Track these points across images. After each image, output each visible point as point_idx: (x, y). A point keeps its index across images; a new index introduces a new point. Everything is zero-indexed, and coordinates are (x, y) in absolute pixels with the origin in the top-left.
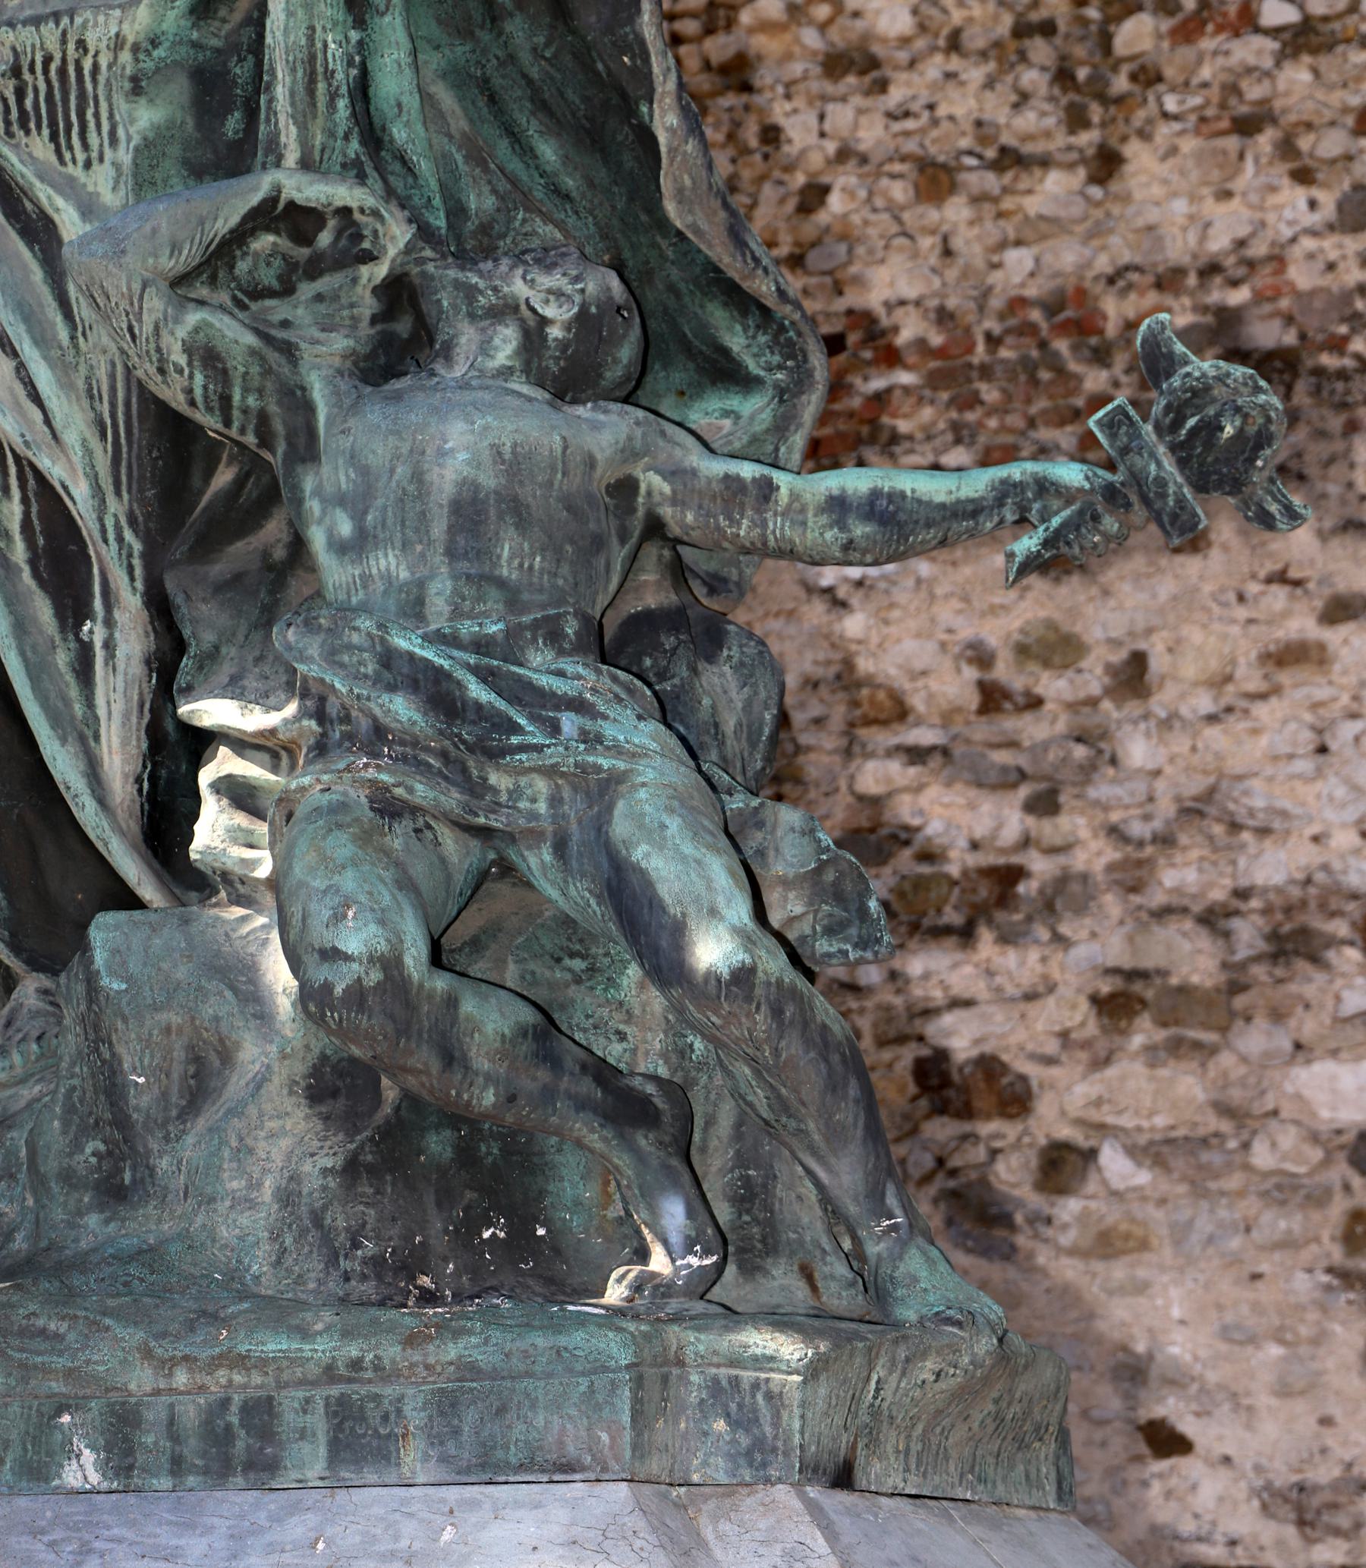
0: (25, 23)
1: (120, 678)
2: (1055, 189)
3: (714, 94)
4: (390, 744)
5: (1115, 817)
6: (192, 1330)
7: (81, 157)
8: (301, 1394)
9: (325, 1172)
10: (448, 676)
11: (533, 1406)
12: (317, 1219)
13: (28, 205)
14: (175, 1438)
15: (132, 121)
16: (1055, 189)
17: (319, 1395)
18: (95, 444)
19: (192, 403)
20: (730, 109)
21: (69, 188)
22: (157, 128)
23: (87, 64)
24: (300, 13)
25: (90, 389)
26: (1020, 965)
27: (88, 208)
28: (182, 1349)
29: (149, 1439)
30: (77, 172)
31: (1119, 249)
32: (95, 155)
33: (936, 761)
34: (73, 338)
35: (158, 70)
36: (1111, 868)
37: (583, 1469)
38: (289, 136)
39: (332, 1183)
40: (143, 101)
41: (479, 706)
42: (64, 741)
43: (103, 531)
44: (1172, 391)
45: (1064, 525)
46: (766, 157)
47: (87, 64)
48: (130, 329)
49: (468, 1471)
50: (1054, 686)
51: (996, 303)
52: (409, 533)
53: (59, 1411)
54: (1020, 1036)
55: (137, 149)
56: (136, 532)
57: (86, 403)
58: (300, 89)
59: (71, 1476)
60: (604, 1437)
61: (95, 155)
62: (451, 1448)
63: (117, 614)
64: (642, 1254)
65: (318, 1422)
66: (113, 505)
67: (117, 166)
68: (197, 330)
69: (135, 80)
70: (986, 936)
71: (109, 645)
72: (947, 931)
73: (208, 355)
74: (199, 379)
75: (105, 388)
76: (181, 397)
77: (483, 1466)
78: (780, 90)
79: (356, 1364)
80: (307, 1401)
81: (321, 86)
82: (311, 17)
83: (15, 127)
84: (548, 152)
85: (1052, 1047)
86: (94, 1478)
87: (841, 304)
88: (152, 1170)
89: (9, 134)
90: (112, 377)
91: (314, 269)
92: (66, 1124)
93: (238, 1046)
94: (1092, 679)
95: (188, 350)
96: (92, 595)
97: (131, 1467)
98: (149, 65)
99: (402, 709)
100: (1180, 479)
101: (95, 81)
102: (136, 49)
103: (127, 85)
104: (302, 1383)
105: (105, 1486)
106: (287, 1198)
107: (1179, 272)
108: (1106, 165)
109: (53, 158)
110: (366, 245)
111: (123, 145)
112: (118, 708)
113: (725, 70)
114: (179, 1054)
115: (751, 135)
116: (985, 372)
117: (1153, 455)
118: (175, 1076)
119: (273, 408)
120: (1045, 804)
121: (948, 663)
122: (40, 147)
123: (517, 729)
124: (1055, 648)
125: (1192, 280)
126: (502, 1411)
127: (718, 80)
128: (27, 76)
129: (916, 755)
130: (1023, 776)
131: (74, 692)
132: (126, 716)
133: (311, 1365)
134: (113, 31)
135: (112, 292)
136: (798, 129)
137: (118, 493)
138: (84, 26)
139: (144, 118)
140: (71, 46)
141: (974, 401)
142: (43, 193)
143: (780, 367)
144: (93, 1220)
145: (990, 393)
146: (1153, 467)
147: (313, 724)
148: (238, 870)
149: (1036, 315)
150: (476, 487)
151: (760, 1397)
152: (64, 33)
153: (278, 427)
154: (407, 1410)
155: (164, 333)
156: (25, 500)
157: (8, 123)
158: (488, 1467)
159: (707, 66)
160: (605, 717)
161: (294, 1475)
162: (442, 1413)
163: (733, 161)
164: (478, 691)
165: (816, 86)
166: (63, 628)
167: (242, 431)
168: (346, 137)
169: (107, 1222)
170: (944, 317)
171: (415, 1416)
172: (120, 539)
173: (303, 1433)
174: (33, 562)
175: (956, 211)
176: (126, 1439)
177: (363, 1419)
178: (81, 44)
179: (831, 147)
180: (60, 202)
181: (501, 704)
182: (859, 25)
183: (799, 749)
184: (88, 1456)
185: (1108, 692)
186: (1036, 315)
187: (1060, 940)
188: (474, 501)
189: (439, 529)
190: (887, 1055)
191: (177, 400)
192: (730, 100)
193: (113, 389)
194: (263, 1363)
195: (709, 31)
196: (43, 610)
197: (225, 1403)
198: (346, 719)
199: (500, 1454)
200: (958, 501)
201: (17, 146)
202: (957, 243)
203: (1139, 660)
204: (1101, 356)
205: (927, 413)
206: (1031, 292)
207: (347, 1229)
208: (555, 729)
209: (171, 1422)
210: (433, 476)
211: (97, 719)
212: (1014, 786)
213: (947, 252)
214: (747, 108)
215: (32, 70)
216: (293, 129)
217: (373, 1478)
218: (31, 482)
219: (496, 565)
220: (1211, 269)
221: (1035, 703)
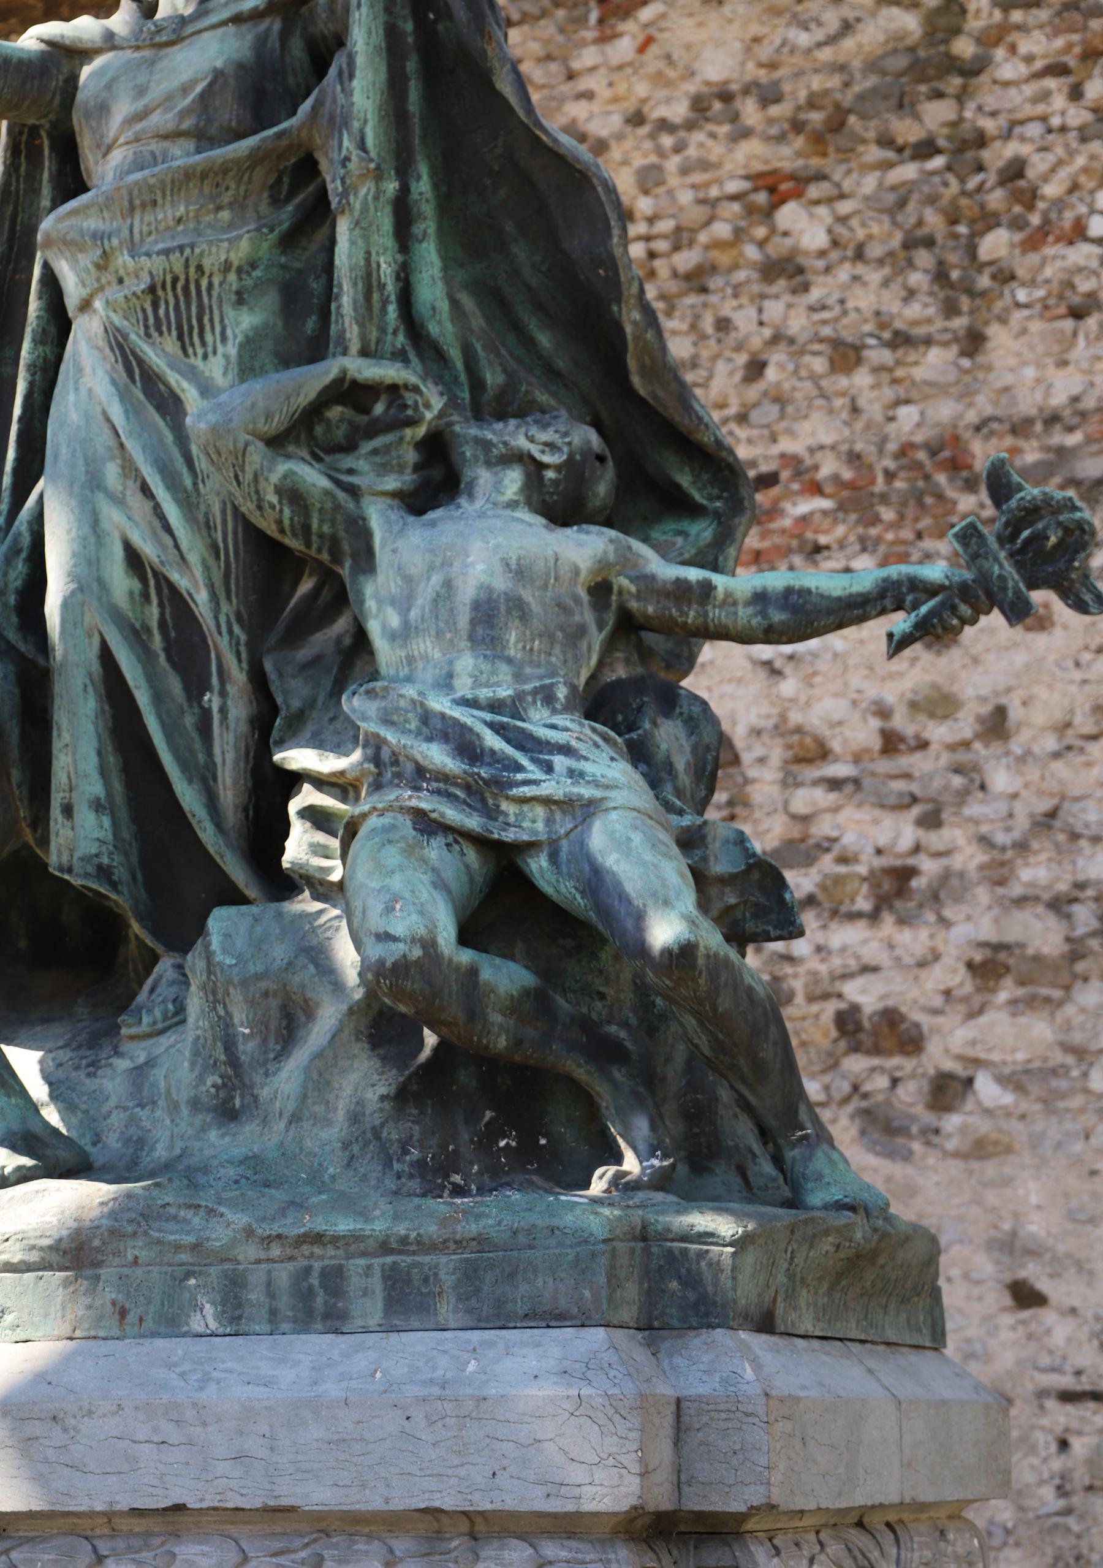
0: (158, 253)
1: (231, 734)
2: (935, 362)
3: (682, 294)
4: (428, 781)
5: (984, 829)
6: (284, 1216)
7: (200, 351)
8: (362, 1262)
9: (383, 1098)
10: (471, 730)
11: (535, 1271)
12: (376, 1133)
13: (162, 387)
14: (271, 1295)
15: (238, 324)
16: (935, 362)
17: (377, 1262)
18: (211, 562)
19: (282, 531)
20: (692, 306)
21: (192, 374)
22: (255, 329)
23: (204, 283)
24: (360, 242)
25: (207, 523)
26: (913, 941)
27: (206, 390)
28: (276, 1229)
29: (252, 1296)
30: (198, 362)
31: (983, 405)
32: (210, 349)
33: (849, 788)
34: (195, 484)
35: (256, 286)
36: (982, 867)
37: (572, 1318)
38: (353, 334)
39: (387, 1105)
40: (245, 309)
41: (493, 752)
42: (190, 781)
43: (218, 626)
44: (1010, 511)
45: (931, 613)
46: (719, 341)
47: (204, 283)
48: (236, 477)
49: (487, 1320)
50: (939, 733)
51: (892, 447)
52: (442, 625)
53: (188, 1275)
54: (914, 993)
55: (241, 345)
56: (242, 627)
57: (205, 532)
58: (361, 298)
59: (196, 1324)
60: (587, 1294)
61: (210, 349)
62: (473, 1302)
63: (229, 688)
64: (618, 1159)
65: (376, 1283)
66: (225, 607)
67: (226, 357)
68: (285, 477)
69: (239, 293)
70: (888, 919)
71: (223, 710)
72: (859, 915)
73: (293, 494)
74: (287, 513)
75: (219, 520)
76: (274, 527)
77: (498, 1316)
78: (729, 291)
79: (404, 1240)
80: (369, 1267)
81: (376, 296)
82: (368, 244)
83: (152, 330)
84: (544, 340)
85: (938, 1001)
86: (213, 1325)
87: (775, 450)
88: (256, 1098)
89: (148, 335)
90: (224, 512)
91: (373, 430)
92: (193, 1064)
93: (318, 1004)
94: (965, 726)
95: (279, 491)
96: (210, 674)
97: (240, 1318)
98: (249, 282)
99: (438, 756)
100: (1016, 577)
101: (210, 296)
102: (239, 270)
103: (233, 297)
104: (364, 1254)
105: (221, 1331)
106: (355, 1118)
107: (1029, 421)
108: (973, 343)
109: (180, 352)
110: (410, 412)
111: (230, 343)
112: (230, 757)
113: (688, 277)
114: (275, 1013)
115: (708, 325)
116: (884, 499)
117: (996, 559)
118: (272, 1028)
119: (342, 534)
120: (931, 821)
121: (857, 715)
123: (520, 768)
124: (939, 704)
125: (1039, 427)
126: (511, 1276)
127: (684, 285)
128: (160, 293)
129: (834, 784)
130: (914, 800)
131: (198, 745)
132: (237, 762)
133: (371, 1241)
134: (223, 257)
135: (223, 450)
136: (744, 319)
137: (229, 598)
138: (202, 255)
139: (244, 321)
140: (192, 270)
141: (876, 520)
142: (173, 378)
143: (719, 498)
144: (213, 1135)
145: (888, 514)
146: (996, 569)
147: (372, 767)
148: (317, 875)
149: (922, 455)
150: (490, 589)
151: (703, 1264)
152: (187, 260)
153: (346, 547)
154: (442, 1275)
155: (261, 479)
156: (161, 605)
157: (146, 327)
158: (500, 1318)
159: (675, 274)
160: (586, 759)
161: (359, 1322)
162: (468, 1278)
163: (695, 344)
164: (492, 741)
165: (756, 288)
166: (189, 699)
167: (319, 550)
168: (395, 333)
169: (223, 1136)
170: (854, 458)
171: (447, 1279)
172: (230, 632)
173: (365, 1293)
174: (167, 650)
175: (862, 379)
176: (236, 1297)
177: (409, 1282)
178: (200, 268)
179: (767, 333)
180: (185, 385)
181: (510, 750)
182: (788, 242)
183: (747, 781)
184: (209, 1309)
185: (978, 736)
186: (922, 455)
187: (945, 923)
188: (489, 600)
189: (463, 620)
190: (815, 1008)
191: (272, 530)
192: (692, 299)
193: (224, 522)
194: (335, 1240)
195: (677, 248)
196: (175, 685)
197: (308, 1270)
198: (396, 763)
199: (510, 1306)
200: (851, 595)
201: (153, 344)
202: (862, 403)
203: (1001, 712)
204: (970, 486)
205: (840, 530)
206: (919, 438)
207: (399, 1141)
208: (549, 768)
209: (269, 1284)
210: (459, 583)
211: (214, 764)
212: (907, 807)
213: (855, 410)
214: (705, 305)
215: (164, 287)
216: (355, 328)
217: (416, 1324)
218: (166, 591)
219: (504, 648)
220: (1052, 419)
221: (923, 745)
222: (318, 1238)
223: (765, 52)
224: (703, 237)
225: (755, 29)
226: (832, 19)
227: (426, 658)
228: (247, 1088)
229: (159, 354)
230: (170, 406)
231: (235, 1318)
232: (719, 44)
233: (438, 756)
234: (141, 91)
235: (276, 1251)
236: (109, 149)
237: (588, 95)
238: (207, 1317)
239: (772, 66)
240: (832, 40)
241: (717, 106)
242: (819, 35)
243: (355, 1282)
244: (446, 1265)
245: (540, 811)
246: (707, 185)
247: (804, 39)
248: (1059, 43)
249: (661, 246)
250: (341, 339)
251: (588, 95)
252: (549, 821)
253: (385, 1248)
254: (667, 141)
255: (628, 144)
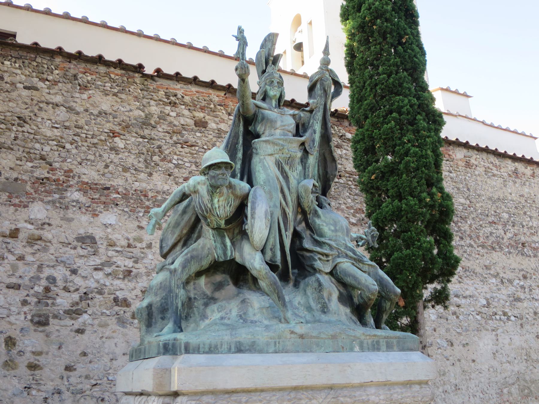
2: (143, 176)
5: (146, 265)
12: (351, 318)
16: (143, 176)
26: (131, 285)
31: (151, 186)
33: (120, 253)
36: (145, 272)
38: (310, 175)
50: (139, 245)
51: (134, 189)
54: (130, 295)
65: (384, 343)
70: (126, 280)
72: (120, 278)
79: (388, 337)
85: (134, 297)
87: (110, 183)
94: (144, 245)
99: (351, 254)
106: (346, 315)
107: (160, 192)
108: (150, 175)
113: (93, 144)
115: (97, 154)
116: (131, 198)
120: (136, 262)
121: (123, 239)
122: (288, 167)
124: (140, 240)
125: (161, 193)
129: (117, 251)
130: (133, 257)
136: (106, 156)
141: (129, 202)
145: (132, 201)
149: (139, 192)
165: (109, 151)
170: (126, 189)
171: (395, 343)
173: (383, 345)
175: (128, 175)
179: (110, 160)
182: (116, 145)
183: (98, 248)
185: (146, 247)
186: (139, 192)
187: (138, 282)
190: (109, 296)
192: (94, 149)
202: (128, 179)
203: (151, 243)
204: (148, 200)
205: (122, 202)
206: (138, 189)
212: (131, 258)
213: (127, 180)
220: (164, 192)
221: (136, 247)
222: (375, 336)
223: (115, 109)
224: (98, 138)
225: (113, 104)
226: (128, 108)
227: (339, 236)
228: (327, 307)
229: (287, 168)
230: (286, 178)
231: (362, 349)
232: (106, 103)
233: (351, 254)
234: (282, 121)
235: (368, 337)
236: (277, 129)
237: (76, 102)
238: (357, 349)
239: (115, 111)
240: (128, 111)
241: (104, 115)
242: (126, 110)
243: (381, 343)
244: (395, 341)
245: (367, 266)
246: (100, 128)
247: (122, 109)
248: (169, 128)
249: (90, 137)
250: (308, 175)
251: (76, 102)
252: (369, 268)
253: (385, 338)
254: (93, 117)
255: (84, 115)
